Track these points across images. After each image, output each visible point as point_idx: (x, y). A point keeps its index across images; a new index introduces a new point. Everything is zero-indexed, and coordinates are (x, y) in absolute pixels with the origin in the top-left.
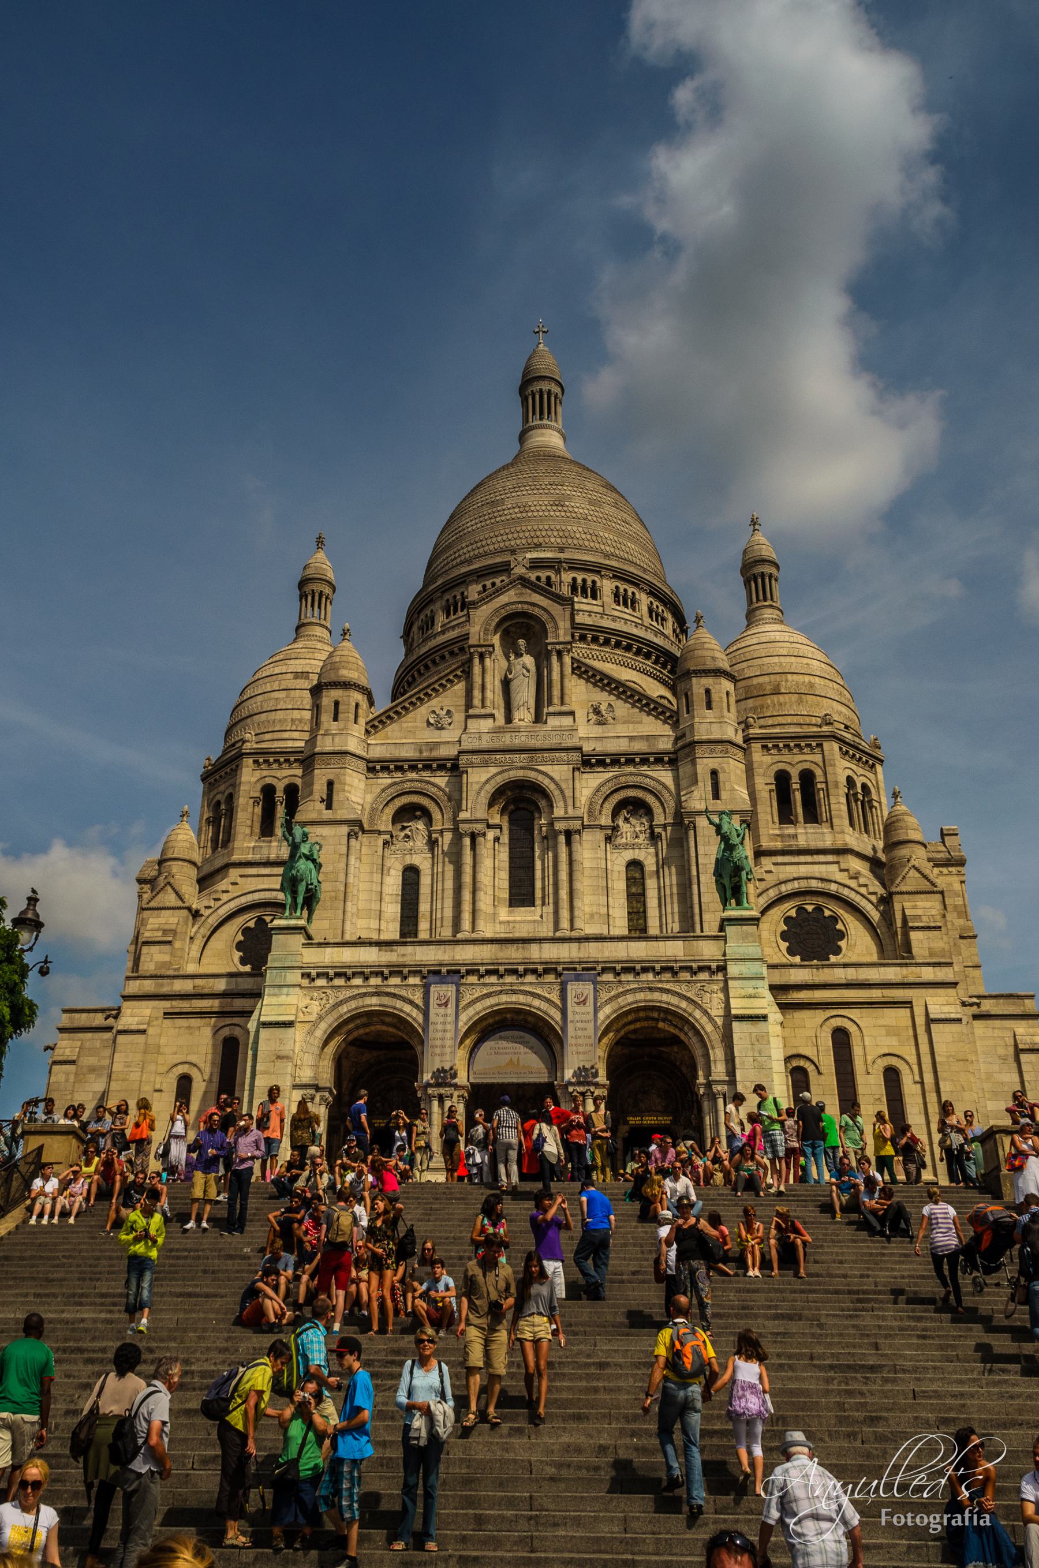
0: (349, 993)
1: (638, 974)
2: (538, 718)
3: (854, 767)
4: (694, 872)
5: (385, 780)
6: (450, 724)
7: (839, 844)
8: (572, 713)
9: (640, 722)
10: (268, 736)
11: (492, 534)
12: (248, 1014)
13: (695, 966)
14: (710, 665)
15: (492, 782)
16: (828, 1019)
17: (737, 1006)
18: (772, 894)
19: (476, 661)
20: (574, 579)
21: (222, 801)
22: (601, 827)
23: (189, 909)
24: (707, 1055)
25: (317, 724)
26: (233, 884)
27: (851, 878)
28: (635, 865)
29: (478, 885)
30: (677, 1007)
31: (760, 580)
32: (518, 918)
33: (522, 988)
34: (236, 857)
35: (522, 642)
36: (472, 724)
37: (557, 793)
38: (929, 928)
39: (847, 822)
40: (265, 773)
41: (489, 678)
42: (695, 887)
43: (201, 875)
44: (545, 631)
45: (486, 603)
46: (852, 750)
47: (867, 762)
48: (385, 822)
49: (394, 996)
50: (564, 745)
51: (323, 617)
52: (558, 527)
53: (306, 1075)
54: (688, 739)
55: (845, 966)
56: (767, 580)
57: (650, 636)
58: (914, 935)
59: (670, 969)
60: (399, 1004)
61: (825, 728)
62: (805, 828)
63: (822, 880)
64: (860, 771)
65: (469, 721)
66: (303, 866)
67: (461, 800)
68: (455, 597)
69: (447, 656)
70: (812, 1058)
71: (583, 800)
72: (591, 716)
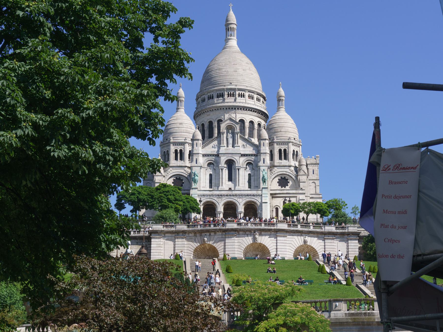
2: (233, 146)
5: (206, 158)
7: (290, 164)
10: (175, 139)
18: (276, 174)
20: (239, 93)
22: (244, 168)
26: (171, 171)
28: (249, 174)
34: (171, 165)
37: (236, 162)
46: (294, 144)
48: (206, 166)
49: (212, 199)
50: (238, 153)
58: (301, 183)
59: (254, 195)
61: (289, 140)
64: (296, 148)
66: (196, 177)
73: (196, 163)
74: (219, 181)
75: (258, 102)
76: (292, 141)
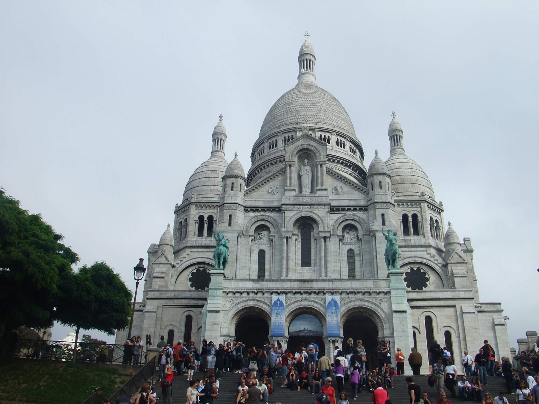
0: (241, 300)
1: (356, 294)
3: (433, 213)
4: (375, 254)
5: (251, 215)
6: (277, 193)
7: (427, 244)
8: (326, 190)
9: (353, 194)
10: (201, 196)
11: (288, 116)
12: (202, 306)
13: (378, 291)
14: (381, 171)
15: (295, 216)
16: (424, 312)
17: (395, 307)
19: (288, 168)
20: (321, 135)
21: (183, 222)
22: (338, 236)
23: (171, 264)
24: (382, 326)
25: (225, 192)
26: (188, 255)
27: (431, 257)
28: (350, 251)
29: (289, 258)
30: (371, 307)
31: (395, 138)
32: (305, 271)
33: (310, 299)
34: (188, 245)
35: (306, 160)
36: (287, 193)
38: (462, 277)
39: (430, 235)
40: (200, 211)
41: (293, 175)
42: (375, 260)
43: (175, 251)
44: (316, 156)
45: (292, 144)
47: (438, 211)
48: (252, 232)
50: (323, 202)
51: (222, 148)
52: (314, 114)
53: (225, 331)
54: (372, 201)
55: (431, 291)
56: (398, 138)
57: (350, 159)
58: (456, 280)
60: (261, 304)
61: (422, 197)
62: (414, 237)
63: (420, 258)
64: (435, 214)
65: (286, 192)
66: (222, 248)
67: (282, 223)
68: (273, 141)
69: (270, 165)
70: (417, 327)
71: (331, 224)
72: (333, 191)
73: (230, 224)
74: (281, 265)
75: (352, 154)
76: (428, 200)
